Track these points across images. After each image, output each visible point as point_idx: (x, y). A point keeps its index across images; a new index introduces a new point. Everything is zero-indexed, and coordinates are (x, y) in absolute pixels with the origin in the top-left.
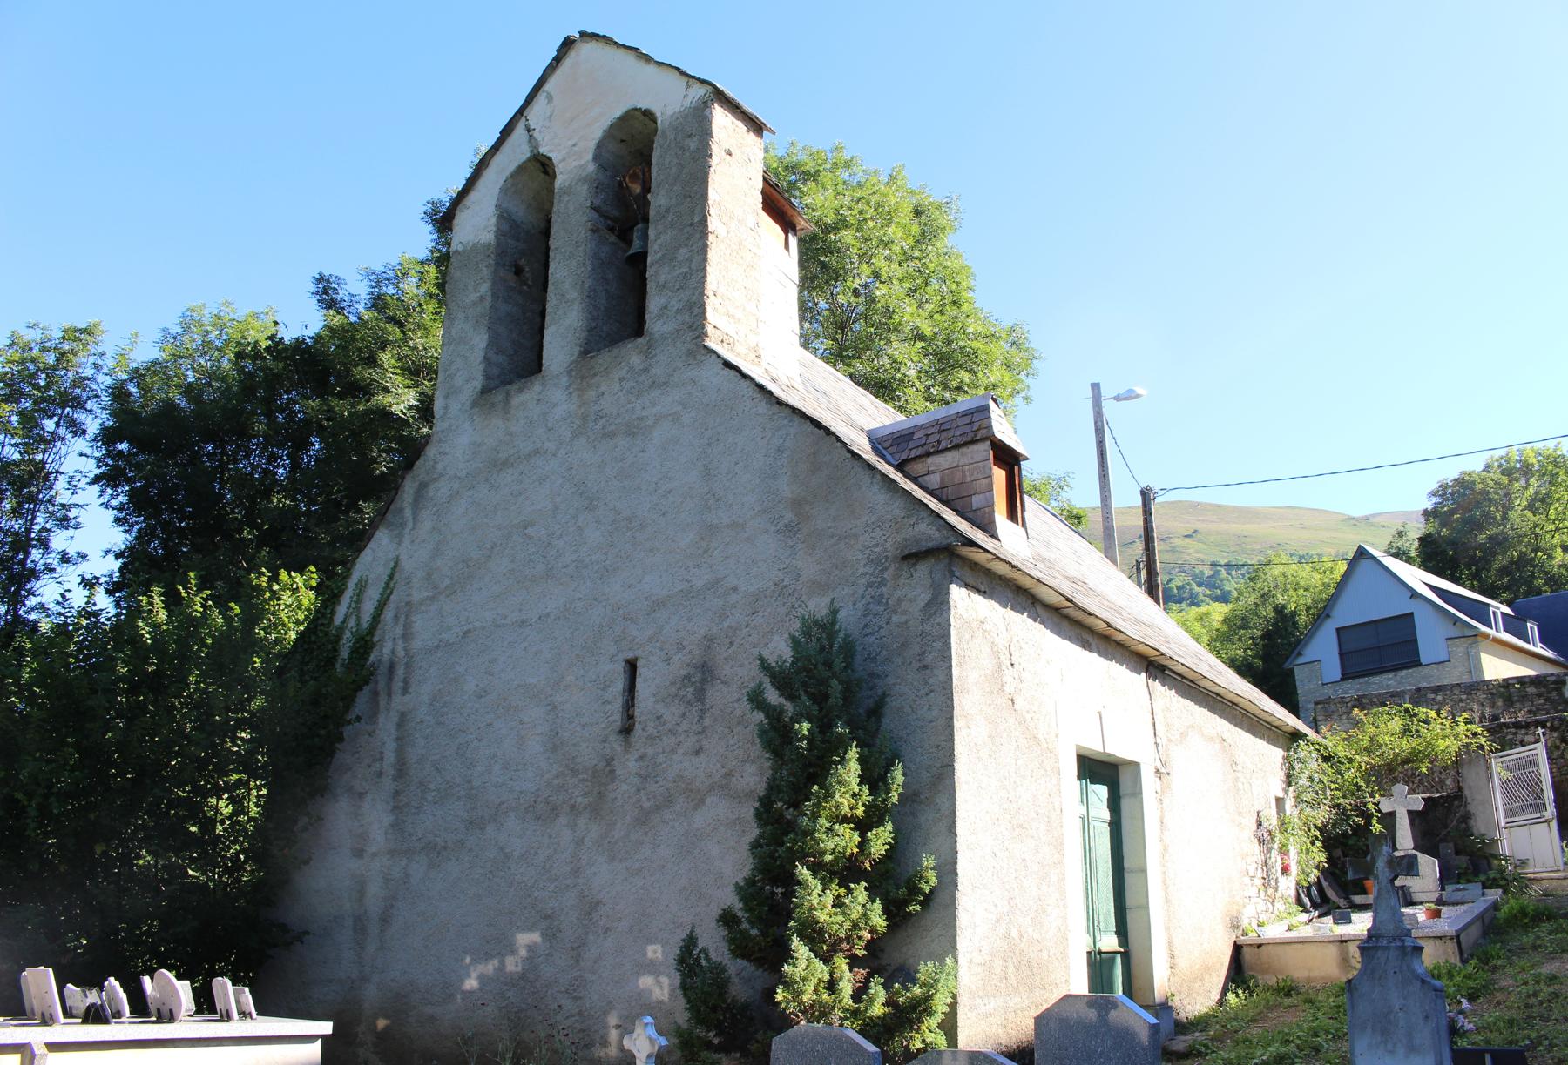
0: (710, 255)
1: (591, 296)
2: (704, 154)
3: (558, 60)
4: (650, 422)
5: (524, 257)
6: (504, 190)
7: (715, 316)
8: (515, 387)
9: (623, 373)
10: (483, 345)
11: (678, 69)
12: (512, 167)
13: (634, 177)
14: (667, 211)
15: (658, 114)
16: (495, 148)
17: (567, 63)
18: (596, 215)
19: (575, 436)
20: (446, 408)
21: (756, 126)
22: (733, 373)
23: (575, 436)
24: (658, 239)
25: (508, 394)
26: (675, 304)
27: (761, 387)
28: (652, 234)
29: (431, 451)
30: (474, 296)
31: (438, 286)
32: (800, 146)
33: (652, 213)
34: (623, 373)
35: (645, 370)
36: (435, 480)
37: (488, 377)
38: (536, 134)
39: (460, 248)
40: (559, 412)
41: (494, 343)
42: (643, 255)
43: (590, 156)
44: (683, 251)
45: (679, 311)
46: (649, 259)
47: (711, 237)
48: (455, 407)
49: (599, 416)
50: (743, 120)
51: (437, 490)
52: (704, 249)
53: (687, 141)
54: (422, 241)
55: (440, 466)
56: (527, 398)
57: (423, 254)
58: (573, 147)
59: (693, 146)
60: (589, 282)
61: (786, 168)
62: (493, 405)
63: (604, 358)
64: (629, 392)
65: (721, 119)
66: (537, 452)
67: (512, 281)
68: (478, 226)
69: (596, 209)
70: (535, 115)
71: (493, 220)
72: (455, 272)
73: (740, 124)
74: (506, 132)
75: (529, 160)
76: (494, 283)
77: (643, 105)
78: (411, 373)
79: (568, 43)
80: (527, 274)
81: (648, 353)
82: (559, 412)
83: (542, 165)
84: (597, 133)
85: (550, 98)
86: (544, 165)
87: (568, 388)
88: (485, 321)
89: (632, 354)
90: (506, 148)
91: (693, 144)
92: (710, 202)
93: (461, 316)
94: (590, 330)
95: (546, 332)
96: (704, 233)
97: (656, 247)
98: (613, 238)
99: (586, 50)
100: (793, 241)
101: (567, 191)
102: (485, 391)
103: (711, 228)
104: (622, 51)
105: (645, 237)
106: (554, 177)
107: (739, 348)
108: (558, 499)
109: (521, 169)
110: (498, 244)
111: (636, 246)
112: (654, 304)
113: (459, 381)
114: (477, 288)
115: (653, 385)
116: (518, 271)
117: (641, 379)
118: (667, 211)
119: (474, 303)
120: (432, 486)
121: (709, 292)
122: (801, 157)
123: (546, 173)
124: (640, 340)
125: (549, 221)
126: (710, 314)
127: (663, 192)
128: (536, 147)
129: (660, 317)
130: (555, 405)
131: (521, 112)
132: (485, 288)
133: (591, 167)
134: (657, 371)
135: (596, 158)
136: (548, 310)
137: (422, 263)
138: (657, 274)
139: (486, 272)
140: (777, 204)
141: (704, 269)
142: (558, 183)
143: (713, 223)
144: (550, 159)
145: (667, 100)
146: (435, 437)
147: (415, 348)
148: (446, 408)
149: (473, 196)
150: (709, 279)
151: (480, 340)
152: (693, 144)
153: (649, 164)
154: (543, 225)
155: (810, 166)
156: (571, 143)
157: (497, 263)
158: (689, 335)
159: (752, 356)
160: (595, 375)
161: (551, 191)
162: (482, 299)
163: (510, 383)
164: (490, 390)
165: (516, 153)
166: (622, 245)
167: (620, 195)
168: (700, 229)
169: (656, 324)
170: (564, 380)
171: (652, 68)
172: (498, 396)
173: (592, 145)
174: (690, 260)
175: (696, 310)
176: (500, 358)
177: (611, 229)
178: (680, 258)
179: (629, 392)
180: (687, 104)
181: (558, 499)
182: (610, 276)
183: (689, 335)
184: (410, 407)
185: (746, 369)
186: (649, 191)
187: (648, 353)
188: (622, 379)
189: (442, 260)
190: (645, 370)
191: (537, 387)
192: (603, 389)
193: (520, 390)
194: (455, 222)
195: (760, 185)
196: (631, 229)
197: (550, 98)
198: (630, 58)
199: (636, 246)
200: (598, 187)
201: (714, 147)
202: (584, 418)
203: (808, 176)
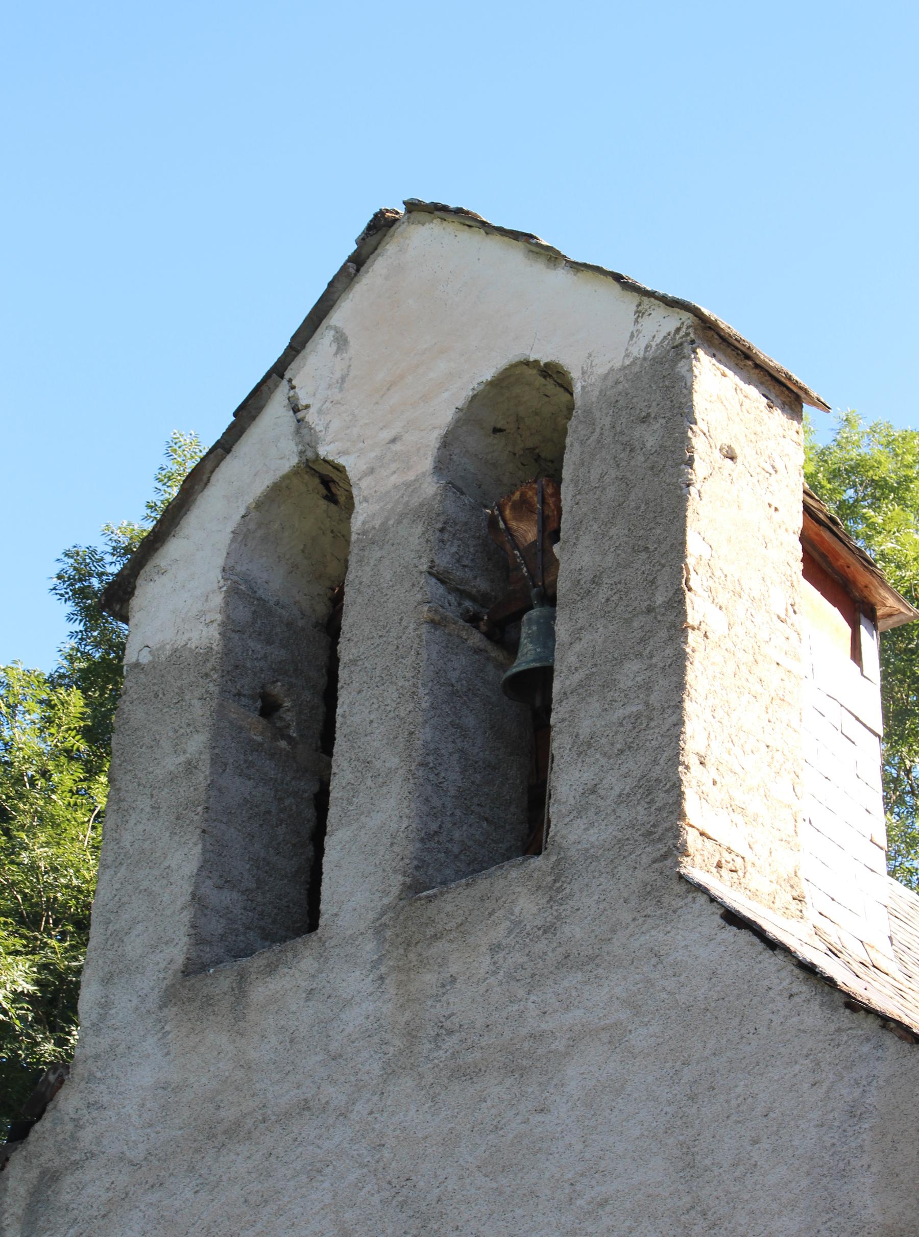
0: (690, 677)
1: (429, 765)
2: (676, 458)
3: (358, 262)
4: (559, 1045)
5: (286, 683)
6: (241, 536)
7: (703, 809)
8: (256, 963)
9: (498, 933)
10: (191, 867)
11: (618, 278)
12: (259, 488)
13: (523, 507)
14: (596, 580)
15: (575, 374)
16: (225, 446)
17: (379, 268)
18: (441, 590)
19: (390, 1072)
20: (105, 1005)
21: (787, 395)
22: (745, 936)
23: (390, 1072)
24: (576, 644)
25: (242, 977)
26: (614, 783)
27: (809, 969)
28: (562, 630)
29: (69, 1101)
30: (172, 763)
31: (87, 734)
32: (864, 426)
33: (563, 586)
34: (498, 933)
35: (549, 929)
36: (77, 1165)
37: (199, 938)
38: (311, 417)
39: (145, 658)
40: (354, 1019)
41: (208, 866)
42: (543, 676)
43: (427, 463)
44: (632, 666)
45: (622, 799)
46: (557, 686)
47: (693, 638)
48: (124, 1003)
49: (443, 1030)
50: (759, 384)
51: (80, 1188)
52: (678, 663)
53: (639, 431)
54: (47, 637)
55: (87, 1135)
56: (286, 986)
57: (49, 662)
58: (392, 440)
59: (651, 442)
60: (425, 734)
61: (835, 475)
62: (208, 1002)
63: (457, 901)
64: (511, 977)
65: (713, 384)
66: (305, 1106)
67: (255, 728)
68: (180, 611)
69: (441, 577)
70: (308, 377)
71: (218, 600)
72: (133, 711)
73: (753, 392)
74: (248, 411)
75: (295, 472)
76: (217, 734)
77: (543, 355)
78: (22, 921)
79: (381, 226)
80: (288, 715)
81: (554, 890)
82: (354, 1019)
83: (326, 483)
84: (442, 413)
85: (341, 341)
86: (326, 482)
87: (375, 965)
88: (196, 816)
89: (517, 891)
90: (246, 446)
91: (650, 437)
92: (690, 561)
93: (144, 803)
94: (427, 838)
95: (330, 843)
96: (678, 628)
97: (572, 659)
98: (476, 639)
99: (420, 238)
100: (870, 644)
101: (377, 538)
102: (193, 969)
103: (692, 618)
104: (495, 244)
105: (548, 635)
106: (349, 506)
107: (755, 880)
108: (349, 1216)
109: (278, 491)
110: (227, 652)
111: (527, 656)
112: (566, 782)
113: (134, 946)
114: (178, 742)
115: (566, 962)
116: (269, 708)
117: (539, 947)
118: (596, 580)
119: (172, 778)
120: (68, 1180)
121: (689, 757)
122: (868, 449)
123: (331, 498)
124: (537, 862)
125: (336, 601)
126: (691, 805)
127: (586, 540)
128: (312, 445)
129: (580, 810)
130: (347, 1004)
131: (279, 371)
132: (197, 744)
133: (430, 488)
134: (575, 931)
135: (440, 467)
136: (335, 793)
137: (53, 682)
138: (574, 718)
139: (199, 711)
140: (834, 566)
141: (679, 706)
142: (357, 522)
143: (697, 608)
144: (340, 469)
145: (594, 345)
146: (79, 1070)
147: (33, 868)
148: (105, 1005)
149: (174, 549)
150: (689, 728)
151: (184, 859)
152: (650, 437)
153: (556, 479)
154: (322, 609)
155: (887, 470)
156: (387, 435)
157: (223, 691)
158: (648, 852)
159: (785, 898)
160: (436, 937)
161: (342, 538)
162: (190, 768)
163: (248, 952)
164: (203, 968)
165: (269, 455)
166: (495, 653)
167: (494, 544)
168: (667, 620)
169: (566, 825)
170: (369, 948)
171: (561, 276)
172: (222, 981)
173: (433, 439)
174: (647, 687)
175: (661, 798)
176: (228, 898)
177: (473, 620)
178: (625, 682)
179: (511, 977)
180: (637, 350)
181: (349, 1216)
182: (470, 721)
183: (648, 852)
184: (18, 997)
185: (774, 930)
186: (555, 536)
187: (554, 890)
188: (495, 948)
189: (100, 674)
190: (549, 929)
191: (308, 963)
192: (453, 969)
193: (271, 969)
194: (135, 603)
195: (797, 521)
196: (516, 617)
197: (341, 341)
198: (515, 255)
199: (527, 656)
200: (446, 529)
201: (698, 443)
202: (411, 1034)
203: (882, 490)
